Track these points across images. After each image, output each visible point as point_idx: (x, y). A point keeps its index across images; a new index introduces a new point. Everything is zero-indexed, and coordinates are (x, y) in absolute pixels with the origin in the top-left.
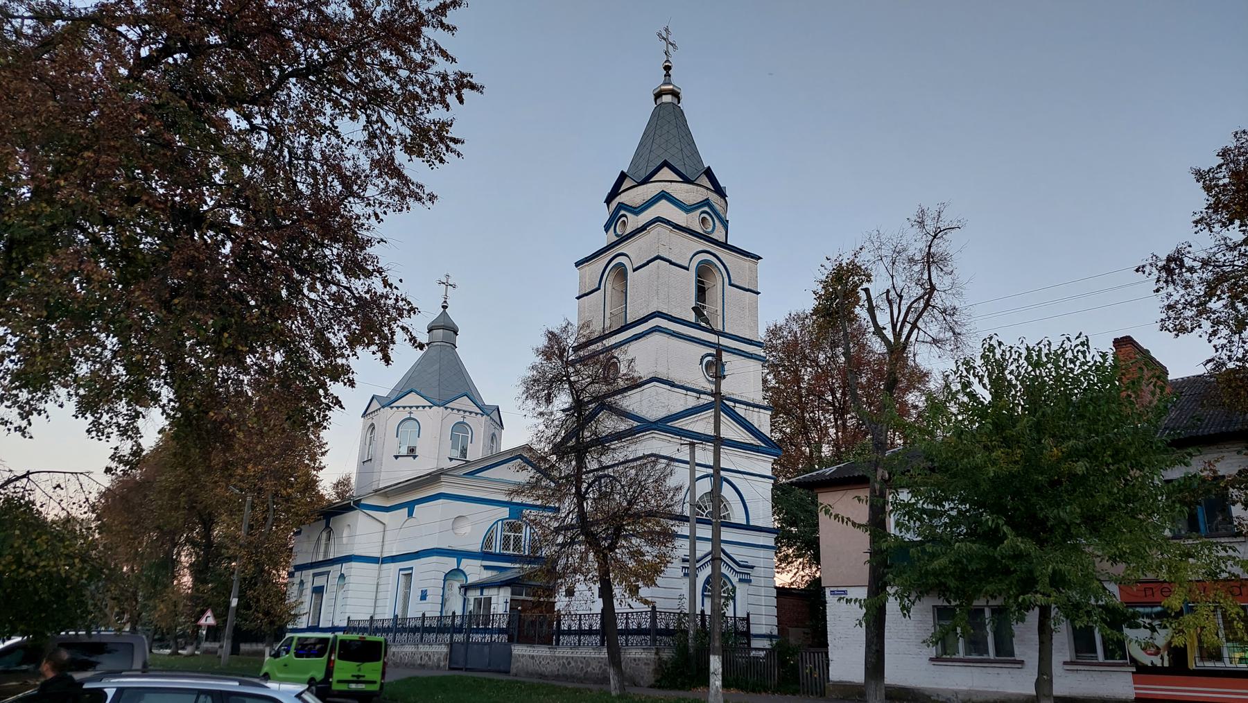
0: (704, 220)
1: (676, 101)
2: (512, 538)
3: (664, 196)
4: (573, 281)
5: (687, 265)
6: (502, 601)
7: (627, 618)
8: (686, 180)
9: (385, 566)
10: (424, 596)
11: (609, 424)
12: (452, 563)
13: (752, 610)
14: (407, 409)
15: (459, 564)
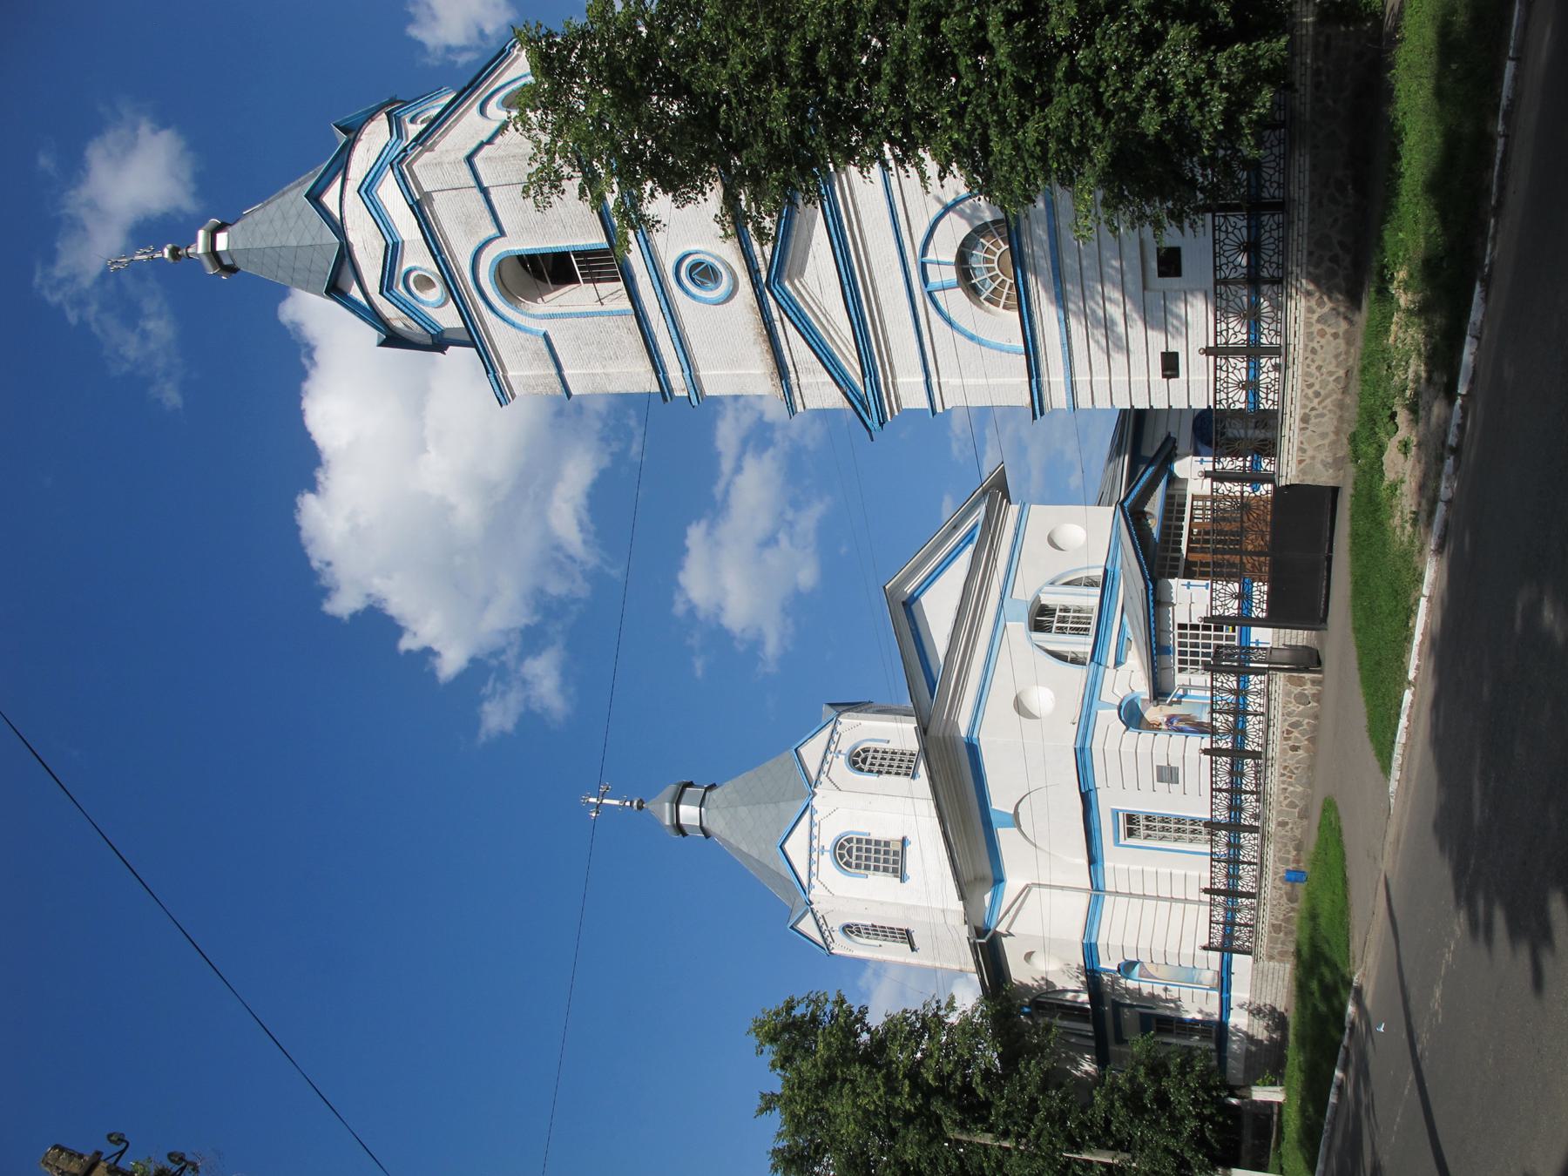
3: (368, 189)
10: (1168, 775)
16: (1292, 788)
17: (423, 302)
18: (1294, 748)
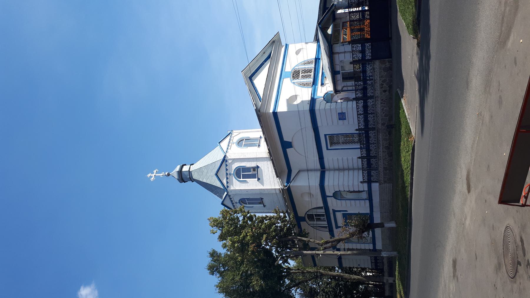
2: (302, 74)
9: (327, 165)
16: (385, 108)
18: (385, 91)
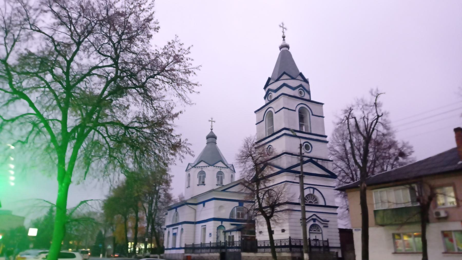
0: (301, 93)
1: (287, 49)
2: (240, 213)
3: (284, 85)
4: (254, 118)
5: (294, 109)
6: (238, 236)
7: (264, 243)
8: (293, 78)
11: (268, 171)
12: (219, 223)
13: (329, 237)
14: (201, 168)
15: (222, 223)
17: (268, 98)
